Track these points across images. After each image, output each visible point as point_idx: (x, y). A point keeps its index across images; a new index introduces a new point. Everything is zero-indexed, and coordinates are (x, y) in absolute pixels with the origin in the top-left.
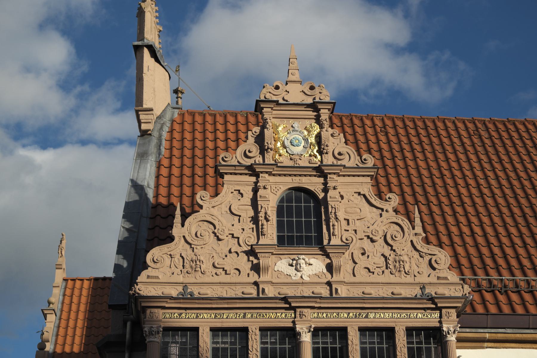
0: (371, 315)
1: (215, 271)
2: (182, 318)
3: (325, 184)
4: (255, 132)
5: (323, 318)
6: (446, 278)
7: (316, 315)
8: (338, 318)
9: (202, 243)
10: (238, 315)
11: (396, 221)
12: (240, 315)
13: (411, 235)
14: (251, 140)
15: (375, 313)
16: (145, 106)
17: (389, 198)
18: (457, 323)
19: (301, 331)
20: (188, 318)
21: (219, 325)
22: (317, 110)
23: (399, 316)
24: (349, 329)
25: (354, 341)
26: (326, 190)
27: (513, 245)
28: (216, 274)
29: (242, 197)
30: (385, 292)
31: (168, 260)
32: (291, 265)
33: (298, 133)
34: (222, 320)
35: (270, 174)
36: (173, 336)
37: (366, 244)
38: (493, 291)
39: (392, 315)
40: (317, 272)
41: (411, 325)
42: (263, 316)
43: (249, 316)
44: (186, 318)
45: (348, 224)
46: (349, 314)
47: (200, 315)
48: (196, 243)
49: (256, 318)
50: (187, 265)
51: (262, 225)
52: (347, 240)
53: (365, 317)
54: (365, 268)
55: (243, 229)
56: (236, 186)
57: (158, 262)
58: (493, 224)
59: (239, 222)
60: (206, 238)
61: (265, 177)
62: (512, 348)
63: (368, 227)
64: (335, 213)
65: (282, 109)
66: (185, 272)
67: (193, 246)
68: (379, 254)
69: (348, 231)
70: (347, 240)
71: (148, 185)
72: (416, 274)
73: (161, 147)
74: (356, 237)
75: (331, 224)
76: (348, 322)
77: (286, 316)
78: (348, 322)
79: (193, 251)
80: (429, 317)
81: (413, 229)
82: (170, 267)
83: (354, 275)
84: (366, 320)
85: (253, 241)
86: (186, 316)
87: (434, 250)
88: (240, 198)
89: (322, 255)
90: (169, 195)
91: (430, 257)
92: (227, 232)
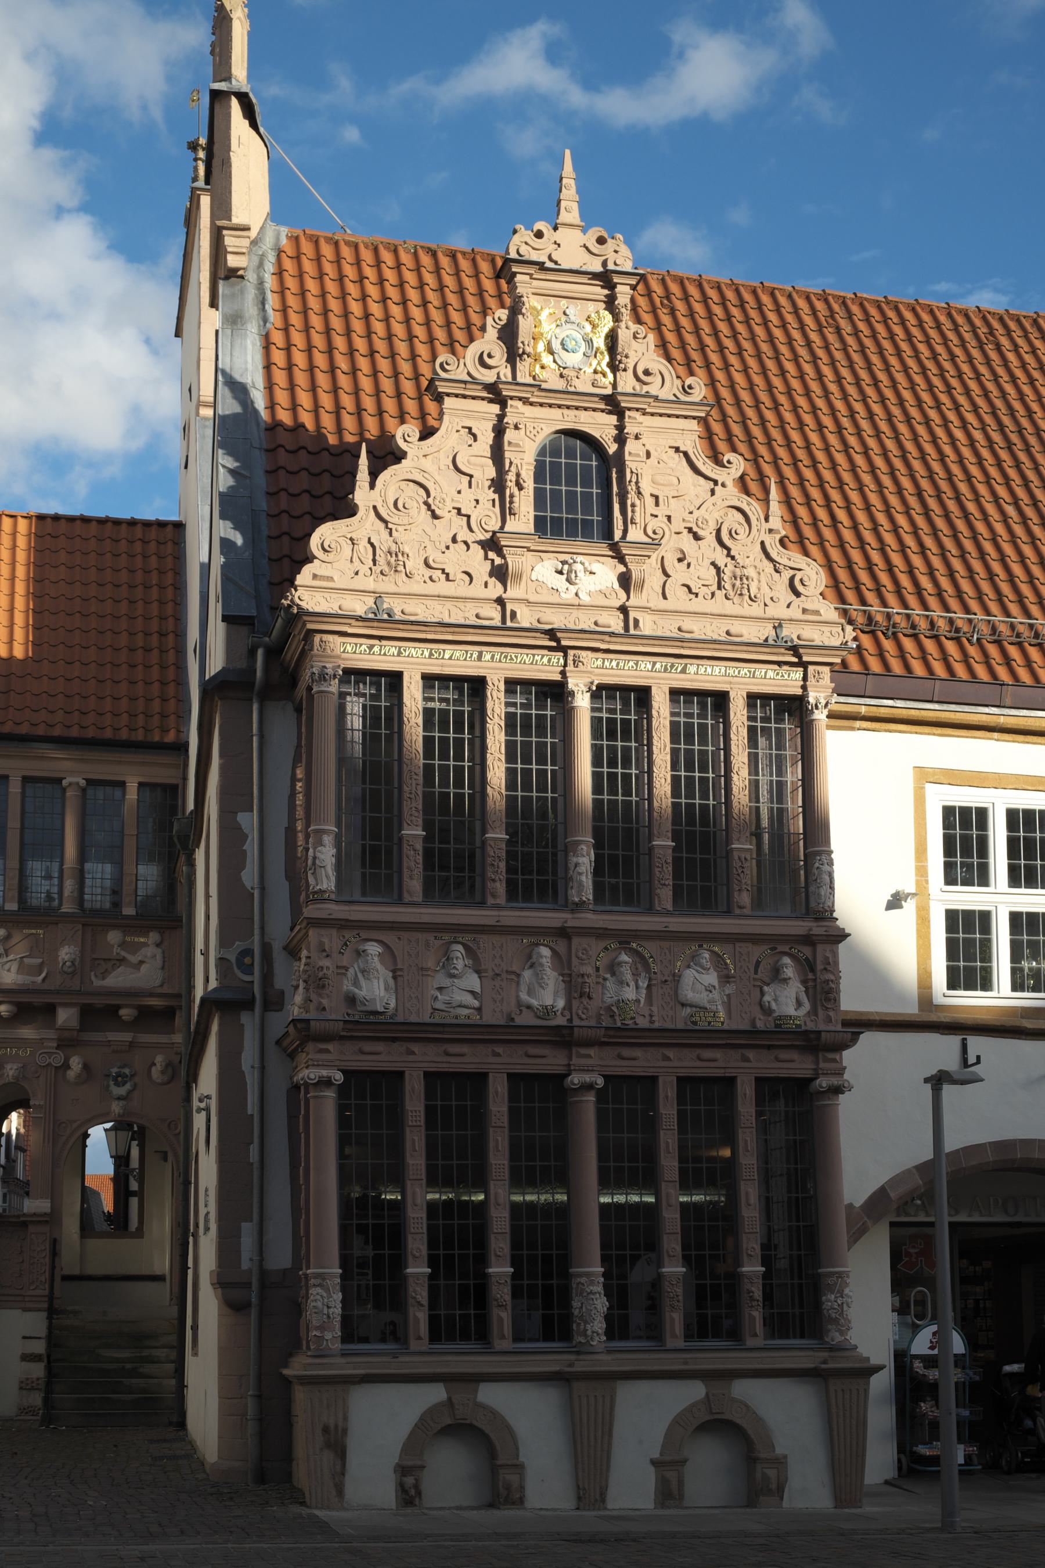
0: (692, 669)
1: (428, 573)
2: (373, 654)
3: (620, 427)
4: (500, 319)
5: (612, 668)
6: (817, 613)
7: (599, 663)
8: (636, 670)
9: (405, 522)
10: (469, 655)
11: (738, 504)
12: (472, 654)
13: (763, 531)
14: (492, 333)
15: (698, 665)
16: (236, 220)
17: (729, 462)
18: (831, 690)
19: (575, 689)
20: (385, 654)
21: (436, 670)
22: (610, 286)
23: (736, 673)
24: (654, 691)
25: (662, 711)
26: (621, 439)
27: (903, 549)
28: (431, 578)
29: (475, 440)
30: (714, 630)
31: (347, 548)
32: (561, 573)
33: (575, 327)
34: (443, 661)
35: (525, 401)
36: (357, 683)
37: (686, 542)
38: (872, 632)
39: (726, 671)
40: (603, 588)
41: (755, 689)
42: (512, 659)
43: (488, 657)
44: (380, 654)
45: (657, 504)
46: (654, 664)
47: (405, 651)
48: (395, 520)
49: (500, 661)
50: (381, 559)
51: (512, 496)
52: (654, 533)
53: (681, 672)
54: (684, 585)
55: (477, 501)
56: (464, 419)
57: (328, 552)
58: (868, 507)
59: (470, 486)
60: (414, 512)
61: (517, 408)
62: (900, 732)
63: (691, 513)
64: (637, 483)
65: (548, 278)
66: (378, 571)
67: (390, 525)
68: (707, 562)
69: (656, 516)
70: (654, 533)
71: (253, 383)
72: (769, 601)
73: (267, 306)
74: (670, 530)
75: (629, 502)
76: (652, 678)
77: (549, 660)
78: (652, 678)
79: (391, 535)
80: (786, 677)
81: (767, 519)
82: (351, 561)
83: (665, 597)
84: (682, 676)
85: (494, 524)
86: (380, 650)
87: (798, 560)
88: (471, 442)
89: (613, 557)
90: (294, 407)
91: (792, 572)
92: (449, 505)
